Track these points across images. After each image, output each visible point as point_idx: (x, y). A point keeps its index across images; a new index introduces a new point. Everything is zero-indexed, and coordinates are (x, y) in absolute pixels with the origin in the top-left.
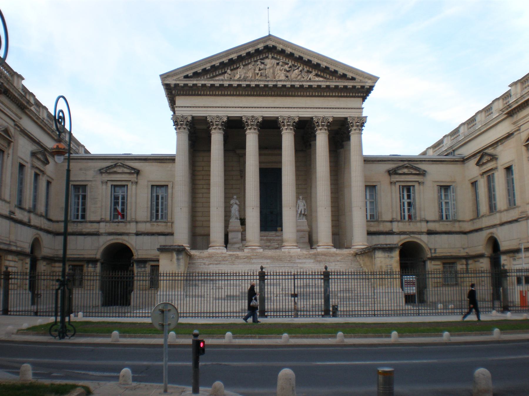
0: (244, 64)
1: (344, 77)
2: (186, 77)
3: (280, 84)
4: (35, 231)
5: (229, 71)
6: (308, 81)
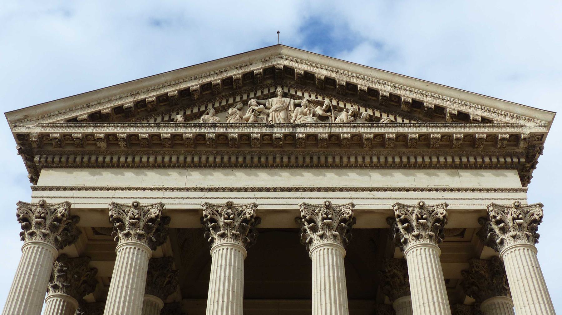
0: (217, 105)
1: (462, 117)
3: (301, 132)
5: (179, 118)
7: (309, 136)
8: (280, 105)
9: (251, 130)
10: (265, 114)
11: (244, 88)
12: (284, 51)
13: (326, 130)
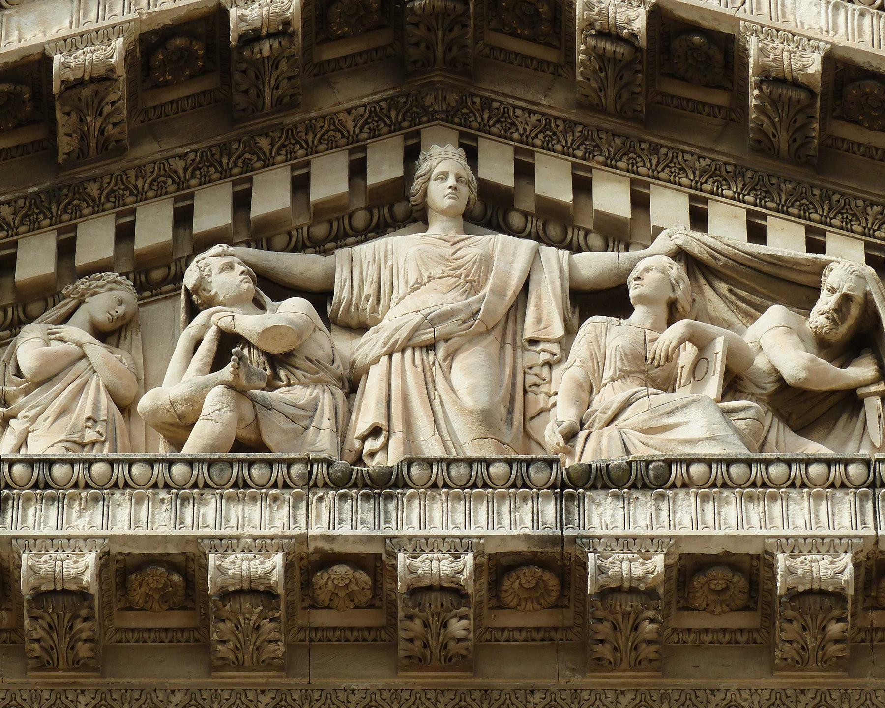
7: (693, 568)
8: (452, 300)
9: (207, 517)
10: (318, 371)
11: (148, 151)
13: (842, 517)
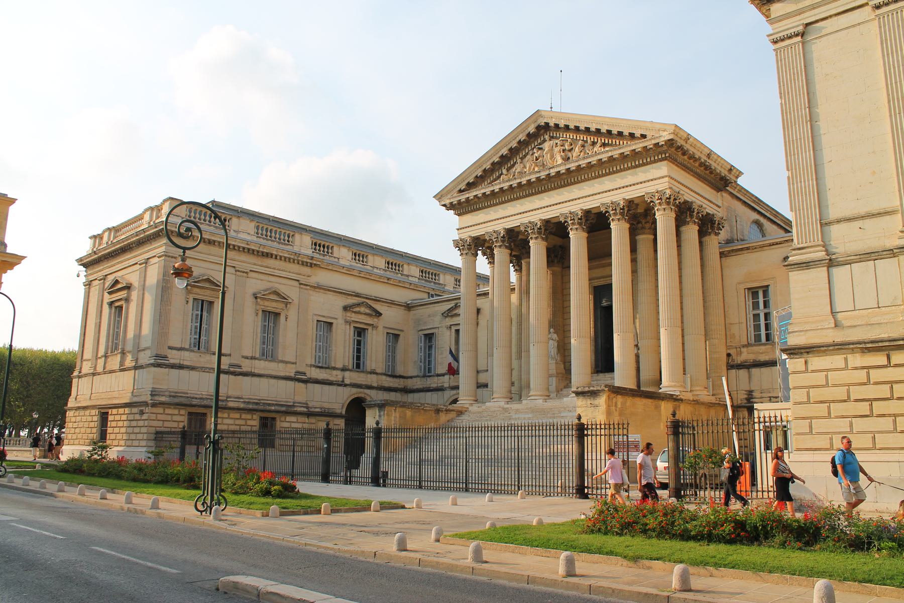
2: (460, 191)
4: (354, 390)
6: (584, 158)
12: (543, 113)
